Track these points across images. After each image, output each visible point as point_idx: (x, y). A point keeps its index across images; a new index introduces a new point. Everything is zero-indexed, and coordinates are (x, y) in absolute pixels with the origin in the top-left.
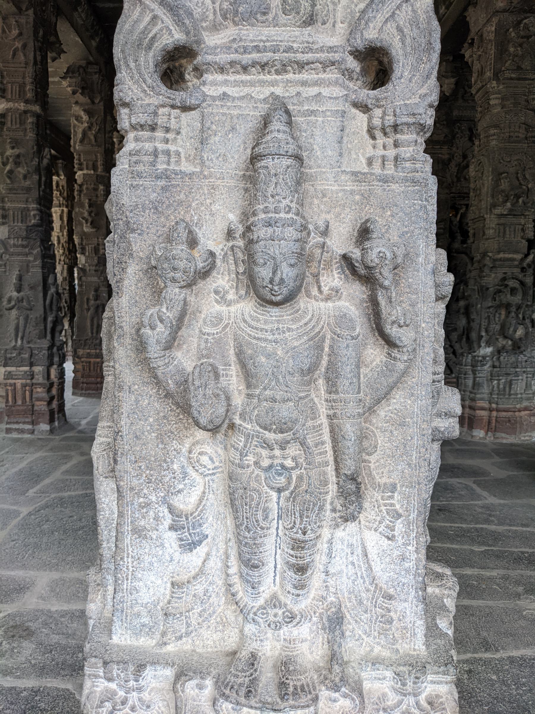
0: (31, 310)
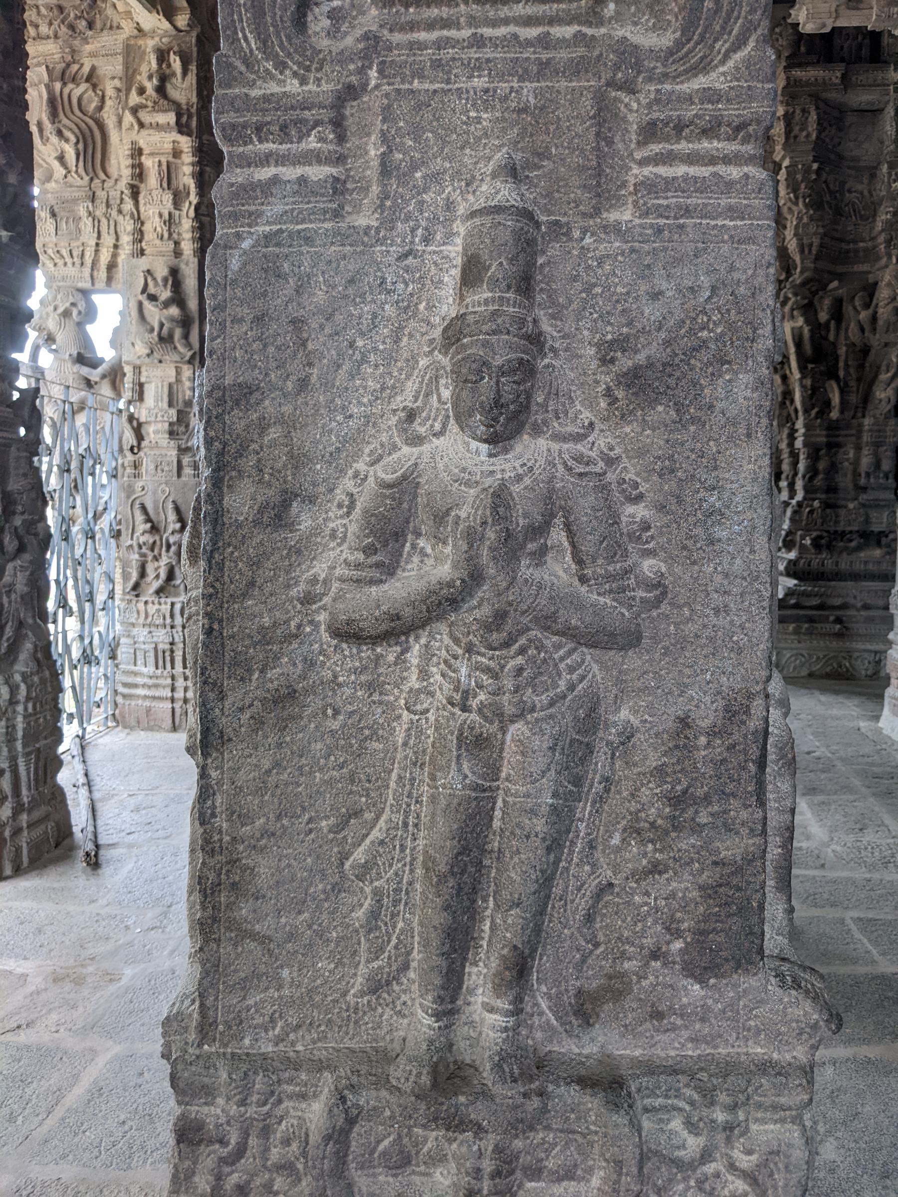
0: (630, 639)
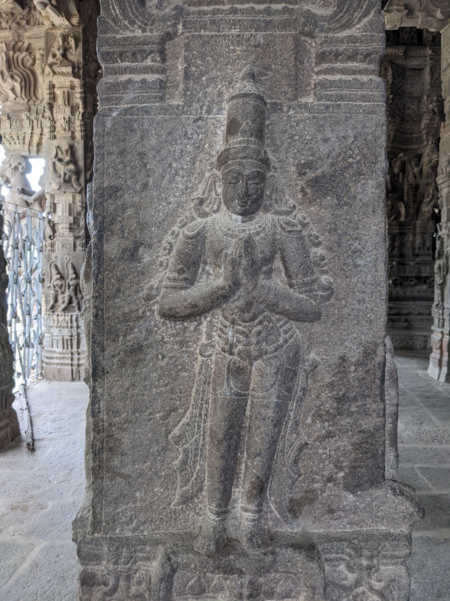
0: (313, 317)
